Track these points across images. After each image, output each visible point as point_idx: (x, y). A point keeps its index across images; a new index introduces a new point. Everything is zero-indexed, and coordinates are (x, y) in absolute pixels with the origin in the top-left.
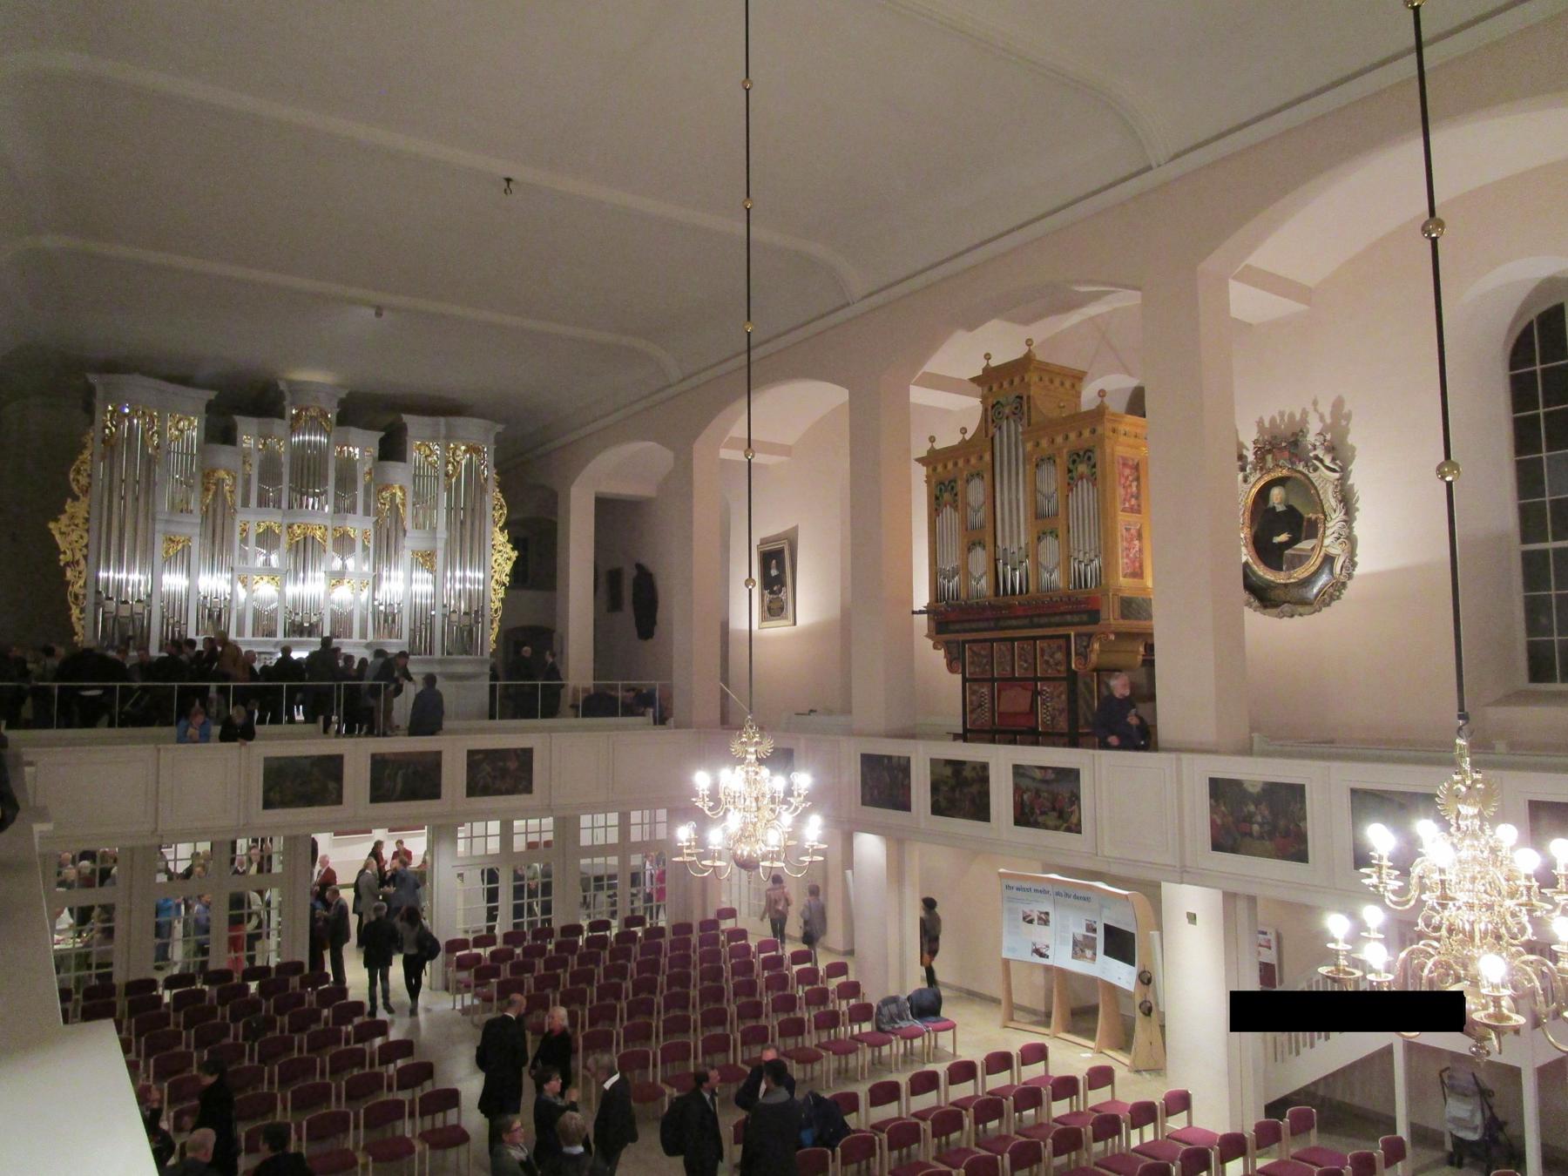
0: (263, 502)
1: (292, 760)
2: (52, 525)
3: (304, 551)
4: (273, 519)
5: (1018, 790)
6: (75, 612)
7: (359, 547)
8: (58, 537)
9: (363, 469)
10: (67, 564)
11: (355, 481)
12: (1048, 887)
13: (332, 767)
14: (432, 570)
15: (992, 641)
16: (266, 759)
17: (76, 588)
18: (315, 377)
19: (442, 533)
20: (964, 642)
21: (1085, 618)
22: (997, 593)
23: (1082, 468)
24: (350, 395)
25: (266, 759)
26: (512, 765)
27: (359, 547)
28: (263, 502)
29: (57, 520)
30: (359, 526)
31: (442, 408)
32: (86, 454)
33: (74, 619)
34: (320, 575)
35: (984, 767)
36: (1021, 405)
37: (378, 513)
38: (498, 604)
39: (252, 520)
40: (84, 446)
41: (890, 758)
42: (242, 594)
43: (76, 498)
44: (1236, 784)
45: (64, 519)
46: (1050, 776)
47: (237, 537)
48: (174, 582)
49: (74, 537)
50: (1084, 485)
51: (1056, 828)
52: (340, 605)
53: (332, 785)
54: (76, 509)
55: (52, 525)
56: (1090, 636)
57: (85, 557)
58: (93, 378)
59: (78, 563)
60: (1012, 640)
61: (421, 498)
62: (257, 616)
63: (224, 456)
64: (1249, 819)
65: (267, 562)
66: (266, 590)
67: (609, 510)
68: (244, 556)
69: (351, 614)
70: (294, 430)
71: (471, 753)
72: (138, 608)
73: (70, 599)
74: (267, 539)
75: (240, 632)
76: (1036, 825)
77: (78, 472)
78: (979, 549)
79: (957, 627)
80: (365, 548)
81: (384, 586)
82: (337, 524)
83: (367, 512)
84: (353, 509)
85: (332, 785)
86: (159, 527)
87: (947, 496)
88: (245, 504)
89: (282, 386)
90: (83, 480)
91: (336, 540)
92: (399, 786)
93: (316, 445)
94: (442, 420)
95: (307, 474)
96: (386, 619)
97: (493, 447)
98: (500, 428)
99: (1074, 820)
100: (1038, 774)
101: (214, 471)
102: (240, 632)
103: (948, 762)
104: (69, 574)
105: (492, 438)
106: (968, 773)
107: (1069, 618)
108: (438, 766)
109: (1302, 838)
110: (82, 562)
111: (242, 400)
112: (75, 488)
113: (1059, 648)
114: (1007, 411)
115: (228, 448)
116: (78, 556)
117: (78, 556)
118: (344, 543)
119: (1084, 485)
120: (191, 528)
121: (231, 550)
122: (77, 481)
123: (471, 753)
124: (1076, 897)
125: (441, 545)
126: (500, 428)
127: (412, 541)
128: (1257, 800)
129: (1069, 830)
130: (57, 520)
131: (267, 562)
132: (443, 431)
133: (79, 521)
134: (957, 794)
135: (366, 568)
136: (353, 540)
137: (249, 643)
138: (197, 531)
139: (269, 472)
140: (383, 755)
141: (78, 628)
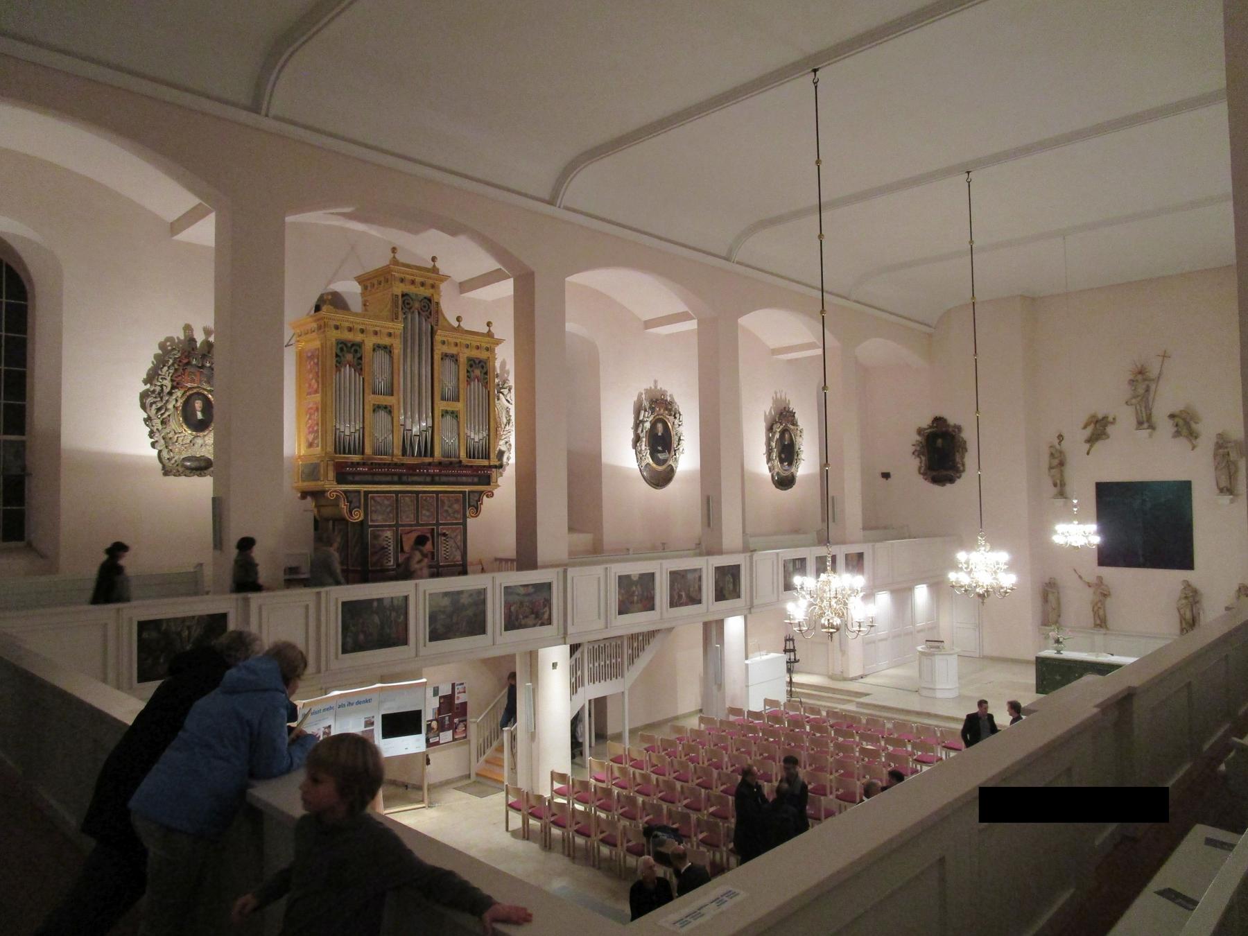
5: (508, 605)
12: (333, 704)
15: (397, 493)
20: (367, 493)
21: (476, 480)
22: (404, 453)
23: (478, 372)
35: (482, 593)
36: (429, 307)
41: (380, 600)
44: (628, 577)
46: (531, 590)
50: (475, 384)
51: (534, 625)
56: (481, 493)
60: (417, 493)
64: (632, 594)
76: (520, 627)
78: (382, 413)
79: (357, 478)
87: (349, 357)
99: (546, 616)
100: (522, 591)
103: (446, 594)
106: (465, 600)
107: (464, 479)
109: (652, 599)
113: (457, 501)
114: (417, 305)
119: (475, 384)
124: (358, 703)
128: (635, 583)
129: (542, 624)
134: (455, 620)
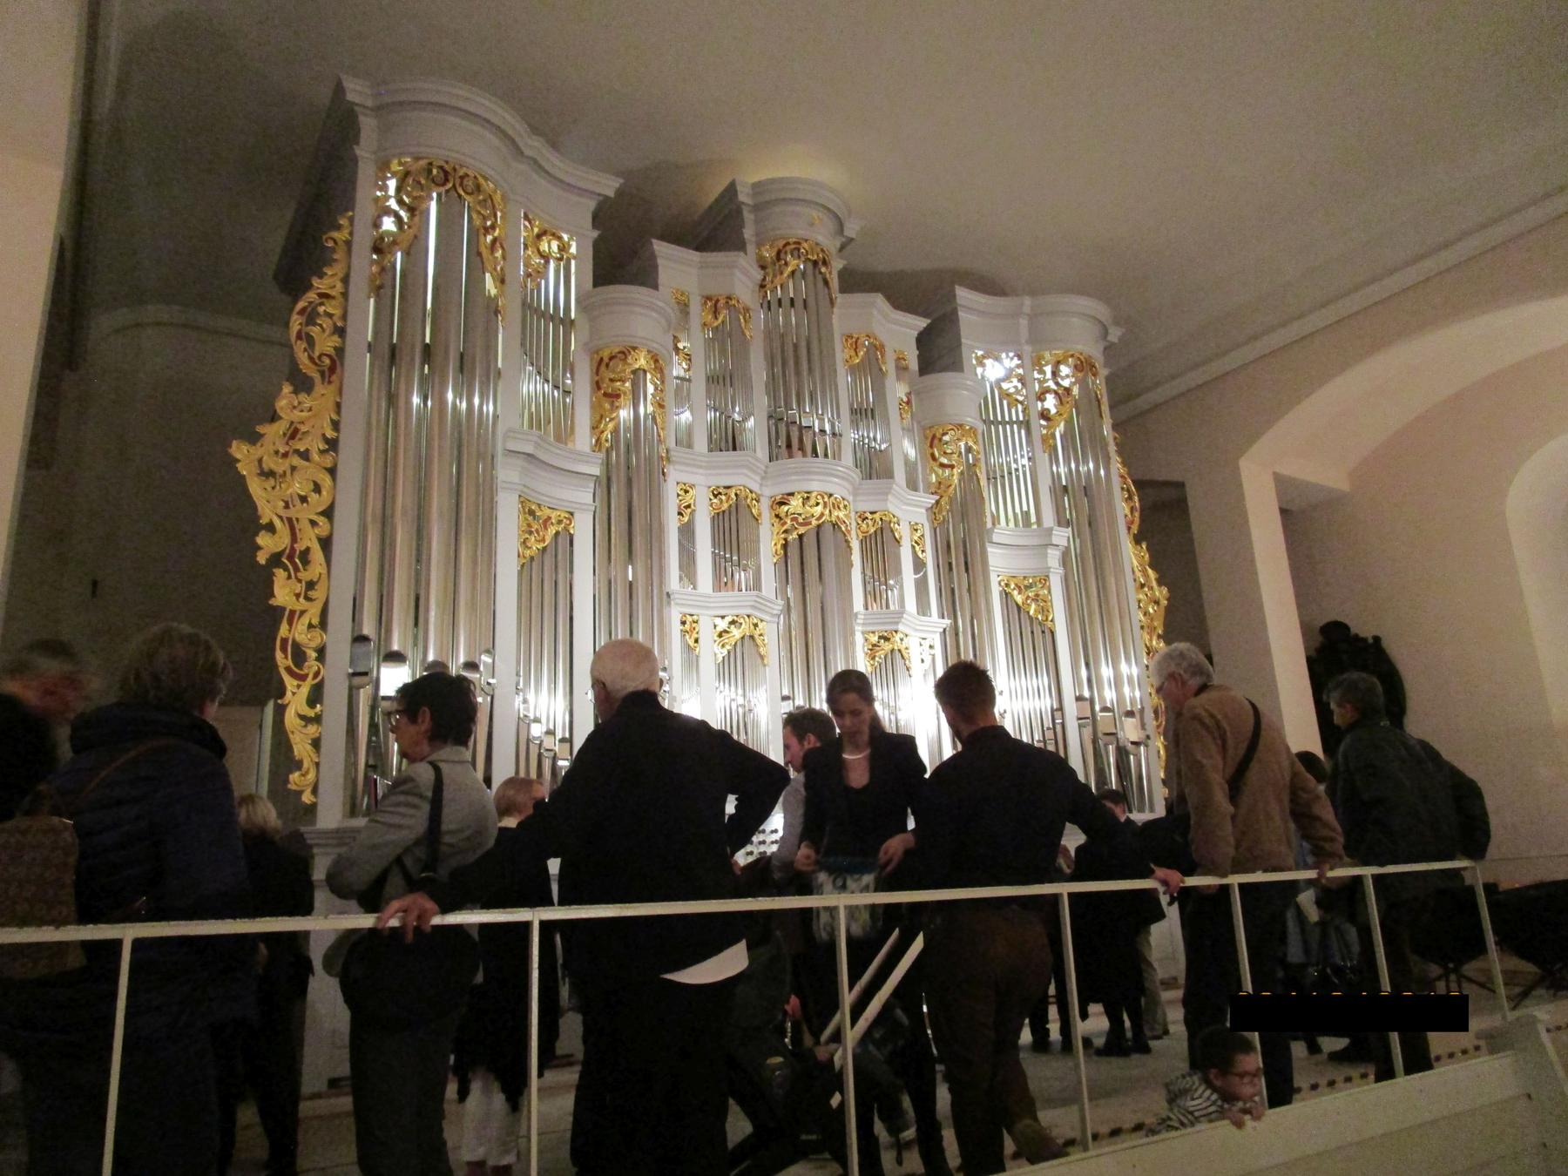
2: (239, 450)
8: (256, 487)
10: (275, 560)
29: (254, 438)
37: (939, 488)
45: (273, 433)
49: (298, 486)
55: (239, 450)
59: (305, 555)
67: (1300, 518)
73: (282, 660)
82: (865, 506)
90: (326, 344)
101: (624, 354)
104: (283, 593)
110: (317, 555)
112: (303, 358)
117: (309, 539)
130: (254, 438)
133: (314, 445)
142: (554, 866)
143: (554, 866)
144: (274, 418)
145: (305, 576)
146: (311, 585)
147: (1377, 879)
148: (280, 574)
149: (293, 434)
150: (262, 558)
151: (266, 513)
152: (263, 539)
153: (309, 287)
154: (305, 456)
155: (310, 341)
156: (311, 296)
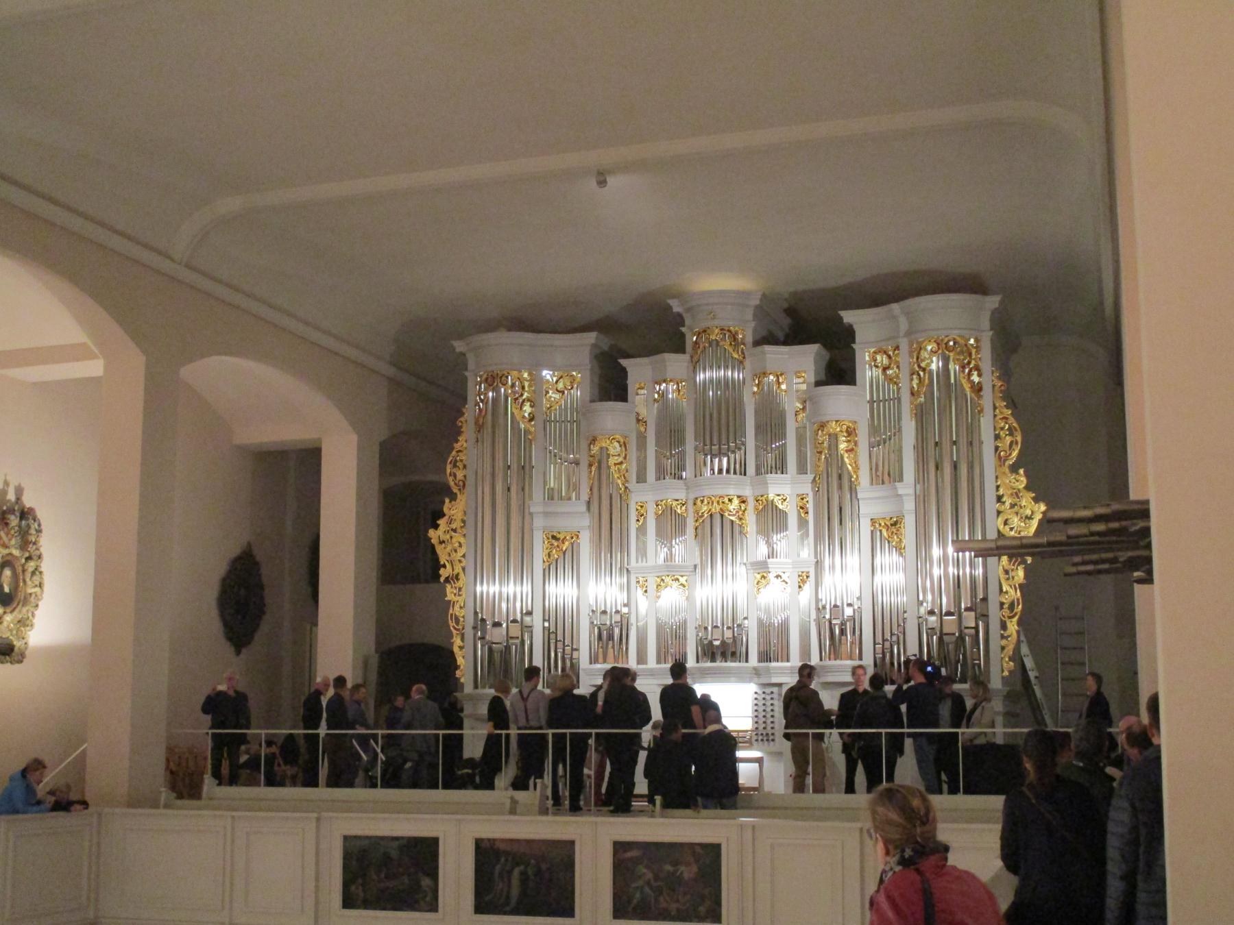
0: (661, 474)
1: (377, 841)
2: (431, 533)
3: (718, 533)
4: (674, 493)
6: (457, 642)
7: (793, 521)
9: (791, 405)
10: (447, 580)
11: (783, 425)
13: (423, 853)
14: (900, 550)
16: (346, 838)
17: (456, 610)
18: (722, 285)
19: (907, 487)
24: (764, 295)
25: (346, 838)
26: (688, 872)
27: (793, 521)
28: (661, 474)
30: (785, 489)
31: (883, 292)
32: (462, 442)
33: (456, 649)
34: (741, 570)
38: (1014, 594)
39: (647, 497)
40: (459, 433)
42: (642, 604)
43: (453, 497)
45: (442, 522)
47: (633, 526)
48: (562, 591)
52: (767, 611)
53: (426, 882)
54: (454, 510)
55: (431, 533)
57: (464, 569)
58: (459, 346)
61: (883, 432)
62: (765, 629)
63: (611, 416)
65: (670, 557)
66: (671, 598)
68: (642, 552)
69: (784, 628)
70: (695, 365)
71: (620, 847)
72: (515, 631)
73: (452, 624)
74: (670, 523)
75: (641, 659)
77: (455, 466)
80: (803, 523)
81: (827, 579)
82: (758, 493)
83: (802, 470)
84: (781, 467)
85: (426, 882)
86: (539, 522)
88: (641, 478)
89: (677, 307)
91: (759, 513)
92: (515, 891)
93: (726, 384)
94: (895, 307)
95: (718, 427)
96: (837, 632)
97: (987, 337)
98: (993, 301)
102: (641, 659)
105: (986, 324)
108: (569, 865)
111: (630, 335)
115: (620, 405)
116: (458, 569)
118: (772, 518)
120: (577, 519)
121: (624, 546)
122: (453, 475)
123: (620, 847)
125: (909, 505)
126: (993, 301)
127: (871, 503)
130: (436, 527)
131: (670, 557)
132: (904, 325)
135: (807, 553)
136: (783, 515)
137: (652, 673)
138: (585, 521)
139: (671, 434)
140: (492, 841)
141: (460, 661)
142: (903, 708)
143: (903, 708)
144: (444, 515)
145: (457, 585)
146: (460, 589)
147: (887, 734)
148: (448, 586)
149: (450, 521)
150: (442, 580)
151: (443, 560)
152: (442, 571)
153: (453, 449)
154: (455, 531)
155: (455, 476)
156: (454, 453)
